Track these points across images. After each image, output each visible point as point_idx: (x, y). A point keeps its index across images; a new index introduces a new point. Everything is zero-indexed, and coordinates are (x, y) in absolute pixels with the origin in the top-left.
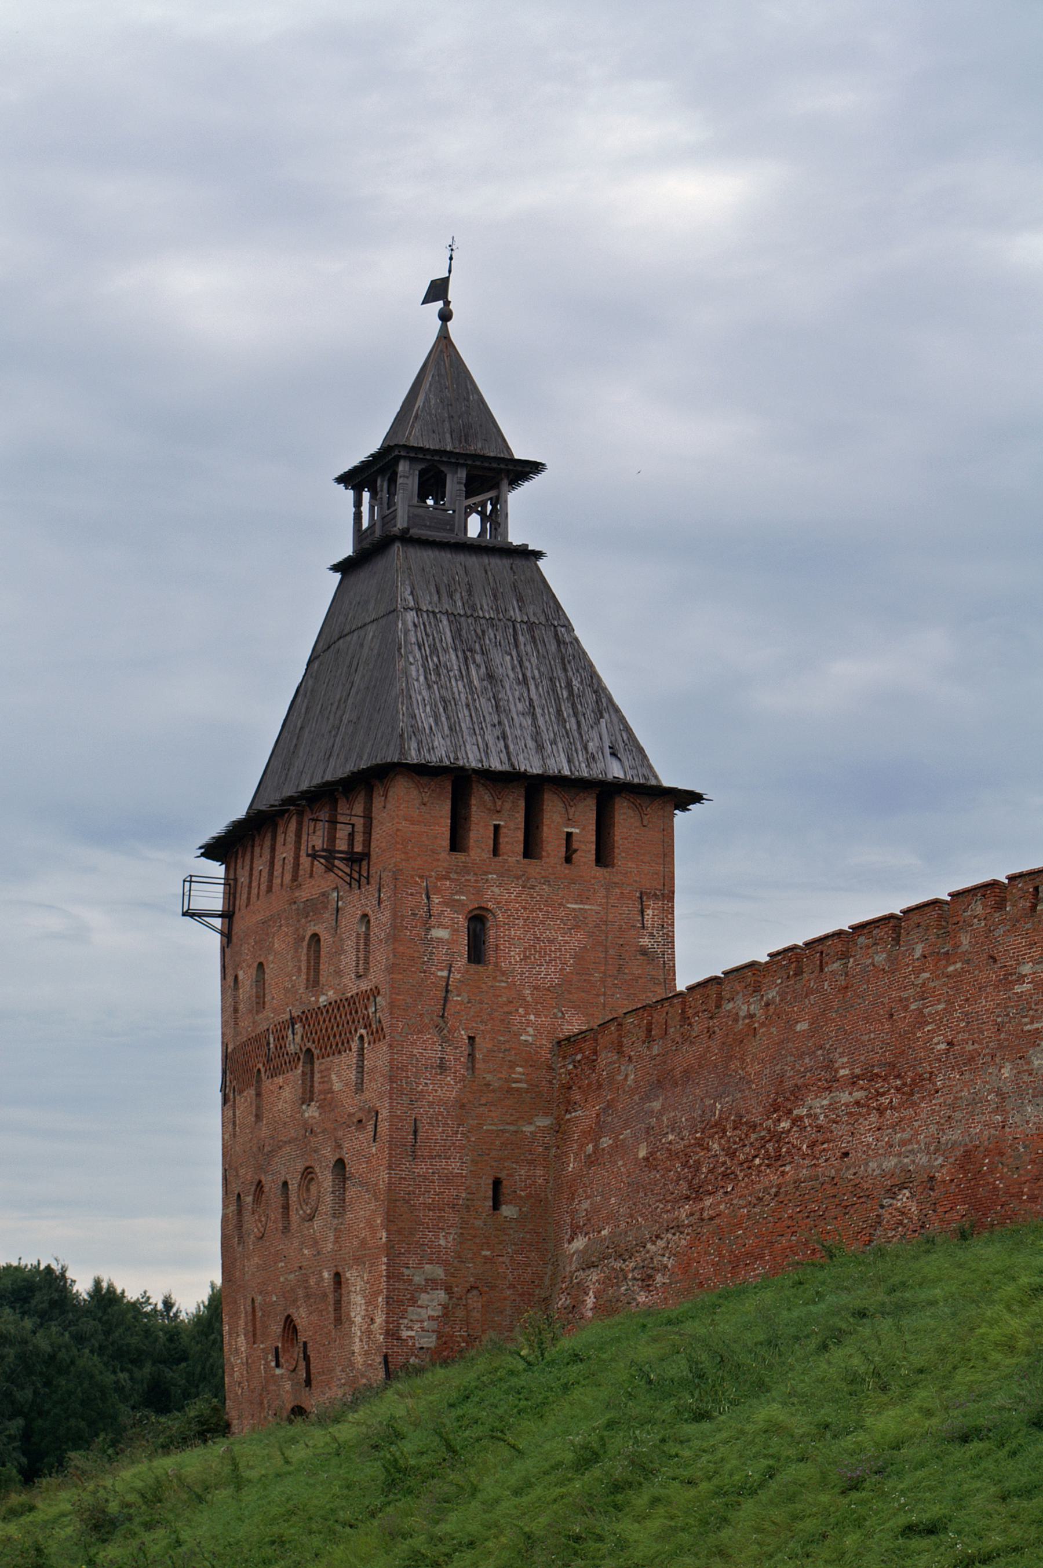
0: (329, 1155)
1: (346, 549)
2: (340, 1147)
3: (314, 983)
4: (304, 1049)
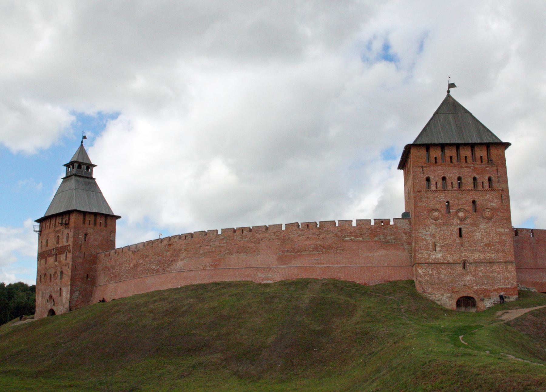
0: (59, 270)
1: (64, 176)
3: (58, 243)
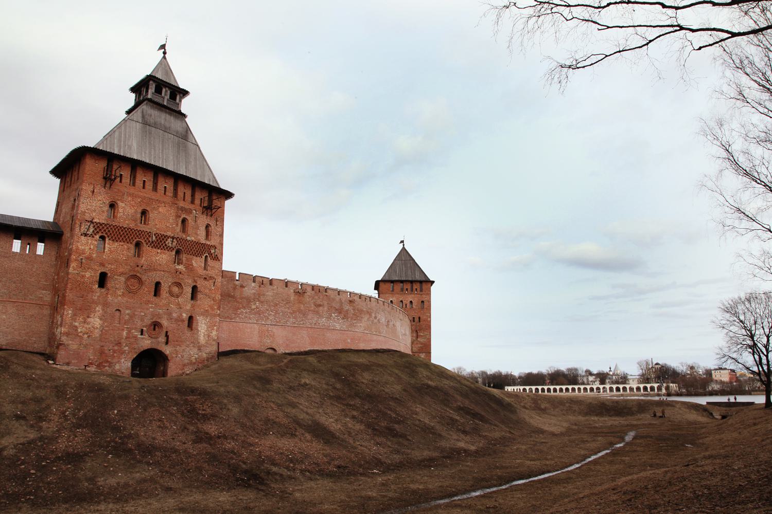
2: (196, 282)
4: (177, 248)
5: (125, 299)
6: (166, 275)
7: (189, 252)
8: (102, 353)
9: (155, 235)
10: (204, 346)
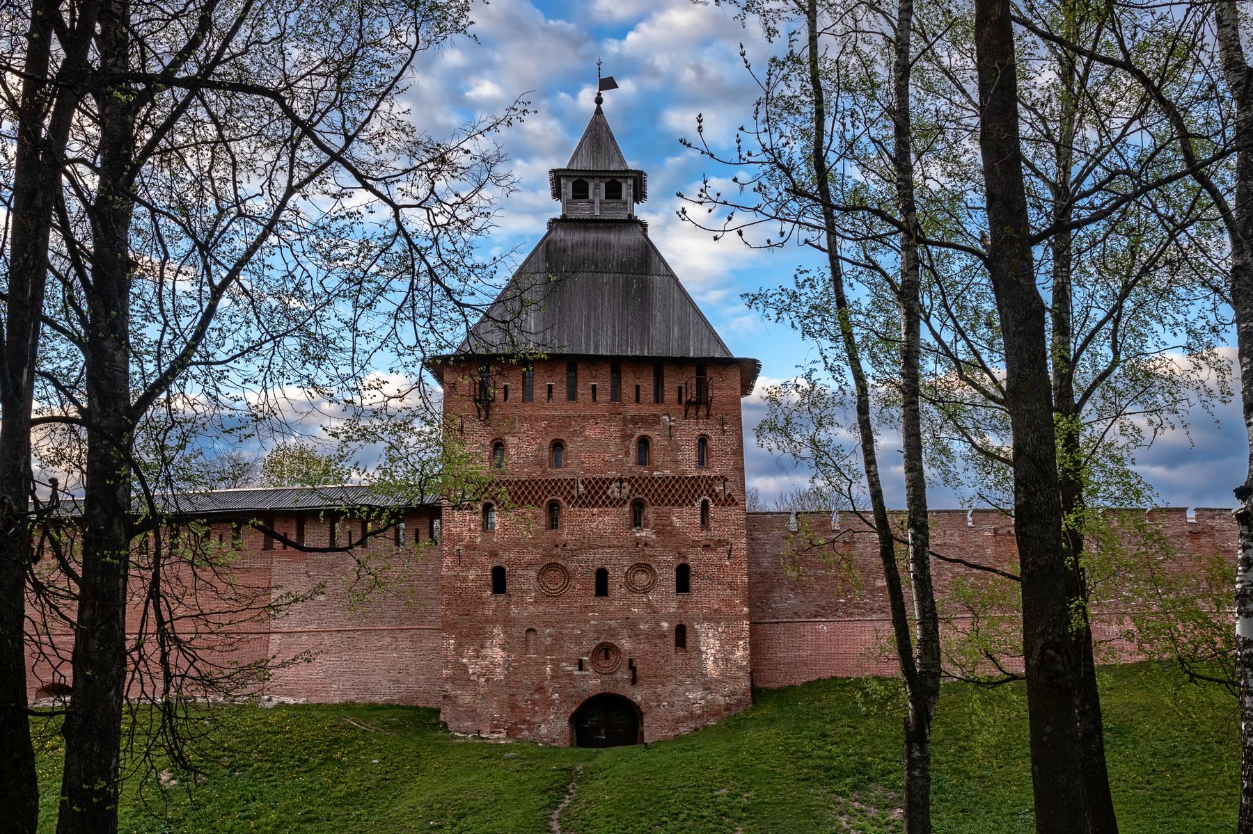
5: (541, 608)
6: (616, 553)
7: (660, 501)
8: (514, 707)
9: (583, 482)
10: (717, 681)
